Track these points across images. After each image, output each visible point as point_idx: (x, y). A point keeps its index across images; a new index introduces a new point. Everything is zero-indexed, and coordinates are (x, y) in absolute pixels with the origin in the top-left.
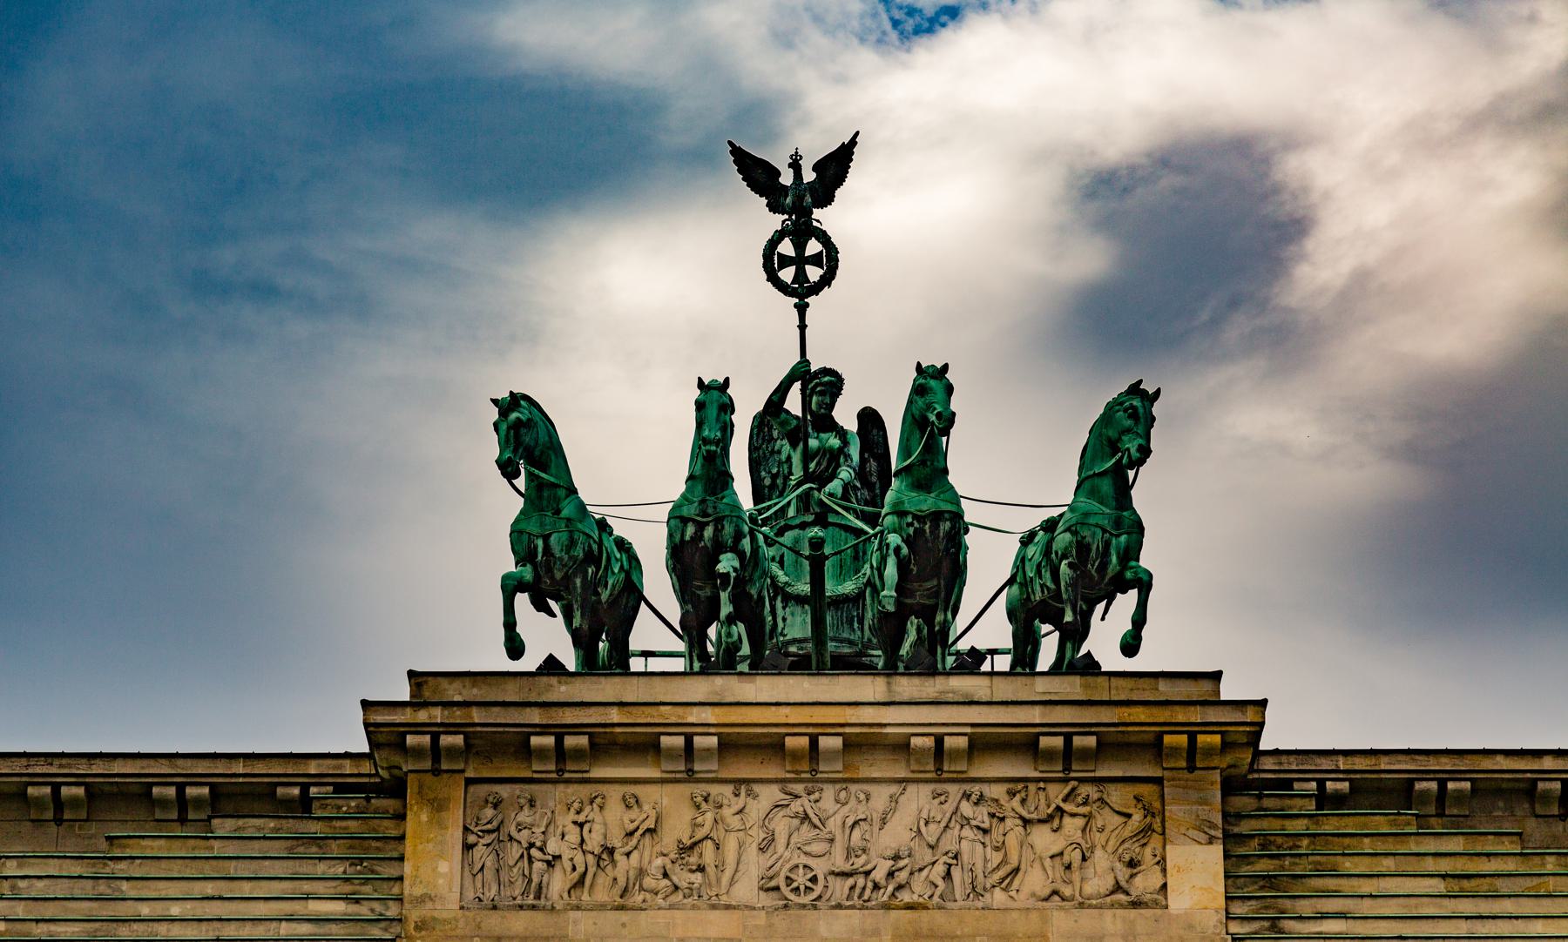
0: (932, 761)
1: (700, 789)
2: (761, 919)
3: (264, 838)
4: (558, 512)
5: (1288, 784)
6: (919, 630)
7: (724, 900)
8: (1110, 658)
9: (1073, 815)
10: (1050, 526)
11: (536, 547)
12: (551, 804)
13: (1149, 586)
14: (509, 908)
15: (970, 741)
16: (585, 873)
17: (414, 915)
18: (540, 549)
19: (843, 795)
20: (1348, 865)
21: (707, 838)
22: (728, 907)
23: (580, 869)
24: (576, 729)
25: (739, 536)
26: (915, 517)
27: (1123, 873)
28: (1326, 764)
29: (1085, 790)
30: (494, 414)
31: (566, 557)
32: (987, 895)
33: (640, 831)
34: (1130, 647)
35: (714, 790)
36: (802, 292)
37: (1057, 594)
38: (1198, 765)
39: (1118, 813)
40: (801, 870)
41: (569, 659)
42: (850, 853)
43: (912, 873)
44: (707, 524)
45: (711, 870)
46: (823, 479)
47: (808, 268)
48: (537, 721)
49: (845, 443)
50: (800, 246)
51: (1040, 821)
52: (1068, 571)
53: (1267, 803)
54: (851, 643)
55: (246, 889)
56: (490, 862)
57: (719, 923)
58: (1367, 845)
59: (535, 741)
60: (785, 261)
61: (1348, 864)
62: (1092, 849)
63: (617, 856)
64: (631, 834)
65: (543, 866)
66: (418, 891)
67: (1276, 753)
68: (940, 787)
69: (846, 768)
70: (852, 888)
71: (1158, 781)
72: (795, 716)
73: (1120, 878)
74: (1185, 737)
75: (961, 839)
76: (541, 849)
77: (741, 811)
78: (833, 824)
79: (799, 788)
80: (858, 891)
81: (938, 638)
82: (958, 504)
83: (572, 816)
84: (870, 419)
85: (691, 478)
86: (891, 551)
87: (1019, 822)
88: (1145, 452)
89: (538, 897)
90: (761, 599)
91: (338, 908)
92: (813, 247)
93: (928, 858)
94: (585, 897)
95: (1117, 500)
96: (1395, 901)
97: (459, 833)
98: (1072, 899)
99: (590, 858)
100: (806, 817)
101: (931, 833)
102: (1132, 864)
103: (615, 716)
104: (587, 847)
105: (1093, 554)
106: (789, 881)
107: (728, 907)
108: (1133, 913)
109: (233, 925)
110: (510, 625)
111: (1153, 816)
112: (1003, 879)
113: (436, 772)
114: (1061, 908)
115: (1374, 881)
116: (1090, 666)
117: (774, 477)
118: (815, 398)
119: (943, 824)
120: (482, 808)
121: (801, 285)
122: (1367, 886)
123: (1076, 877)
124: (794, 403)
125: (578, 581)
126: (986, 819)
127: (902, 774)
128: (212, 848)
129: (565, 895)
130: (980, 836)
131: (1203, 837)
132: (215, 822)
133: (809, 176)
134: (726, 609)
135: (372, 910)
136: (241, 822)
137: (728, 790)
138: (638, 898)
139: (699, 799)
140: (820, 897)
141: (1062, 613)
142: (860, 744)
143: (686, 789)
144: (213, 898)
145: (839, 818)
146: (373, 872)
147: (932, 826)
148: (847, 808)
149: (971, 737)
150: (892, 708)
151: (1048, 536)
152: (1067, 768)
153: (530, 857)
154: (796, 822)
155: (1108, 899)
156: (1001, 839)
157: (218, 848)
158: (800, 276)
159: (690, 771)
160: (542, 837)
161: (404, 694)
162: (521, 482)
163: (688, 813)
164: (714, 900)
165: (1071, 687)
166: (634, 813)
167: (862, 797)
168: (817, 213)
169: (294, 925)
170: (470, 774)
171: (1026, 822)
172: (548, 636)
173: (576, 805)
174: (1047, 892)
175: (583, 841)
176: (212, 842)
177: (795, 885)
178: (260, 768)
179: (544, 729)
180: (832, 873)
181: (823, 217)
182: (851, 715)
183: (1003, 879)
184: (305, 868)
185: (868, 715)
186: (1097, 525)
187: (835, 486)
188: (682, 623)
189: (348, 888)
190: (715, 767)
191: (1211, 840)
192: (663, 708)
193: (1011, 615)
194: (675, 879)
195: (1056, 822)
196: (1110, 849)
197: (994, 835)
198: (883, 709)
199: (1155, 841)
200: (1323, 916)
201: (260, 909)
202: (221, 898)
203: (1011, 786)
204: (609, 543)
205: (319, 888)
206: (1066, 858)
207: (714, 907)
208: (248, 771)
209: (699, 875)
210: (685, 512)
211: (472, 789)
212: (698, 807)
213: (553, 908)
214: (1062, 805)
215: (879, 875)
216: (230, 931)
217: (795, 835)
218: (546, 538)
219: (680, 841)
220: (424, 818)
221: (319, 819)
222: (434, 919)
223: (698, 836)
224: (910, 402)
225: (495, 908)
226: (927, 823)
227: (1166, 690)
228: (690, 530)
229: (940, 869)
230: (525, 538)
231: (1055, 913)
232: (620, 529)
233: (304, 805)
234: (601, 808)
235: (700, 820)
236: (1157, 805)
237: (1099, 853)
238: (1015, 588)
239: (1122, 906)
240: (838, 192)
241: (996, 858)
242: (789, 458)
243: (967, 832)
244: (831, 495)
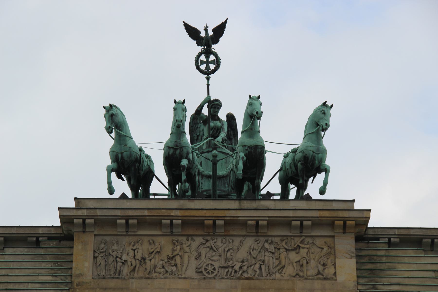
0: (254, 229)
1: (175, 238)
2: (196, 282)
3: (23, 254)
4: (126, 145)
5: (378, 239)
6: (249, 186)
7: (183, 276)
8: (316, 195)
9: (304, 248)
10: (294, 151)
11: (118, 157)
12: (124, 243)
13: (329, 171)
14: (109, 278)
15: (268, 222)
16: (136, 266)
17: (76, 281)
18: (120, 157)
19: (224, 240)
20: (400, 267)
21: (177, 254)
22: (185, 278)
23: (134, 265)
24: (132, 217)
25: (188, 153)
26: (249, 147)
27: (321, 268)
28: (391, 232)
29: (307, 240)
30: (104, 111)
31: (129, 160)
32: (274, 275)
33: (155, 252)
34: (322, 192)
35: (180, 238)
36: (208, 73)
37: (297, 175)
38: (347, 231)
39: (319, 248)
40: (210, 266)
41: (129, 194)
42: (226, 260)
43: (248, 267)
44: (177, 149)
45: (179, 266)
46: (215, 136)
47: (210, 64)
48: (119, 215)
49: (223, 125)
50: (207, 57)
51: (292, 250)
53: (371, 245)
54: (225, 191)
55: (17, 272)
56: (103, 263)
57: (181, 284)
58: (406, 260)
59: (119, 221)
60: (202, 63)
61: (400, 266)
62: (310, 260)
63: (147, 261)
64: (152, 253)
65: (121, 264)
66: (78, 272)
67: (374, 228)
68: (257, 238)
69: (225, 231)
70: (227, 272)
71: (333, 237)
72: (208, 213)
75: (264, 256)
76: (120, 258)
77: (189, 246)
78: (221, 250)
79: (209, 238)
80: (229, 273)
81: (256, 188)
82: (263, 143)
83: (131, 247)
84: (231, 118)
85: (172, 133)
86: (241, 158)
87: (284, 250)
88: (327, 125)
89: (119, 275)
90: (195, 175)
91: (49, 278)
92: (212, 58)
93: (254, 262)
94: (136, 275)
95: (318, 142)
96: (417, 279)
97: (92, 252)
98: (303, 277)
99: (137, 262)
100: (211, 248)
102: (324, 265)
103: (146, 213)
105: (309, 160)
106: (206, 269)
107: (185, 278)
108: (325, 282)
109: (12, 285)
110: (109, 183)
111: (331, 248)
112: (279, 270)
113: (84, 232)
114: (300, 280)
115: (409, 272)
116: (308, 198)
117: (198, 136)
118: (212, 109)
119: (258, 251)
120: (101, 244)
121: (208, 71)
122: (407, 274)
123: (305, 269)
124: (205, 111)
125: (133, 168)
126: (273, 249)
127: (244, 234)
128: (5, 258)
129: (129, 274)
130: (271, 255)
131: (348, 256)
132: (6, 249)
133: (211, 33)
134: (184, 177)
135: (61, 279)
136: (15, 249)
137: (184, 238)
138: (154, 275)
139: (175, 241)
140: (216, 275)
141: (299, 180)
142: (231, 223)
143: (170, 238)
144: (5, 275)
145: (223, 248)
146: (62, 266)
147: (255, 251)
148: (225, 245)
150: (241, 211)
151: (294, 154)
152: (301, 232)
153: (116, 261)
154: (208, 249)
155: (316, 277)
156: (278, 256)
157: (7, 258)
158: (208, 67)
159: (172, 232)
160: (121, 254)
161: (73, 205)
162: (113, 135)
163: (171, 247)
164: (180, 276)
165: (302, 204)
166: (152, 246)
167: (231, 241)
168: (213, 46)
169: (34, 284)
170: (96, 233)
171: (287, 250)
172: (122, 187)
173: (133, 243)
174: (294, 274)
175: (135, 255)
176: (5, 256)
177: (208, 271)
178: (22, 231)
179: (122, 218)
180: (220, 267)
181: (215, 47)
182: (227, 213)
183: (279, 270)
184: (38, 265)
185: (233, 213)
186: (311, 150)
187: (219, 139)
188: (169, 183)
189: (53, 272)
190: (180, 230)
191: (351, 258)
192: (163, 210)
193: (281, 181)
194: (166, 268)
195: (297, 251)
196: (316, 260)
197: (276, 255)
198: (238, 211)
199: (332, 257)
200: (391, 284)
201: (22, 279)
202: (8, 275)
203: (282, 238)
204: (143, 156)
205: (43, 271)
206: (301, 263)
207: (180, 278)
208: (17, 232)
209: (175, 267)
210: (170, 145)
211: (97, 237)
212: (174, 244)
213: (124, 278)
214: (299, 244)
215: (237, 268)
216: (11, 287)
217: (208, 254)
218: (122, 153)
219: (168, 256)
220: (80, 247)
221: (42, 248)
222: (83, 282)
223: (175, 253)
224: (247, 108)
225: (104, 278)
226: (253, 250)
227: (335, 206)
228: (172, 151)
229: (257, 266)
230: (115, 153)
231: (297, 281)
232: (147, 151)
233: (38, 243)
235: (175, 248)
236: (332, 245)
237: (312, 261)
238: (282, 172)
239: (321, 279)
240: (221, 39)
241: (277, 262)
242: (203, 130)
243: (267, 253)
244: (218, 142)
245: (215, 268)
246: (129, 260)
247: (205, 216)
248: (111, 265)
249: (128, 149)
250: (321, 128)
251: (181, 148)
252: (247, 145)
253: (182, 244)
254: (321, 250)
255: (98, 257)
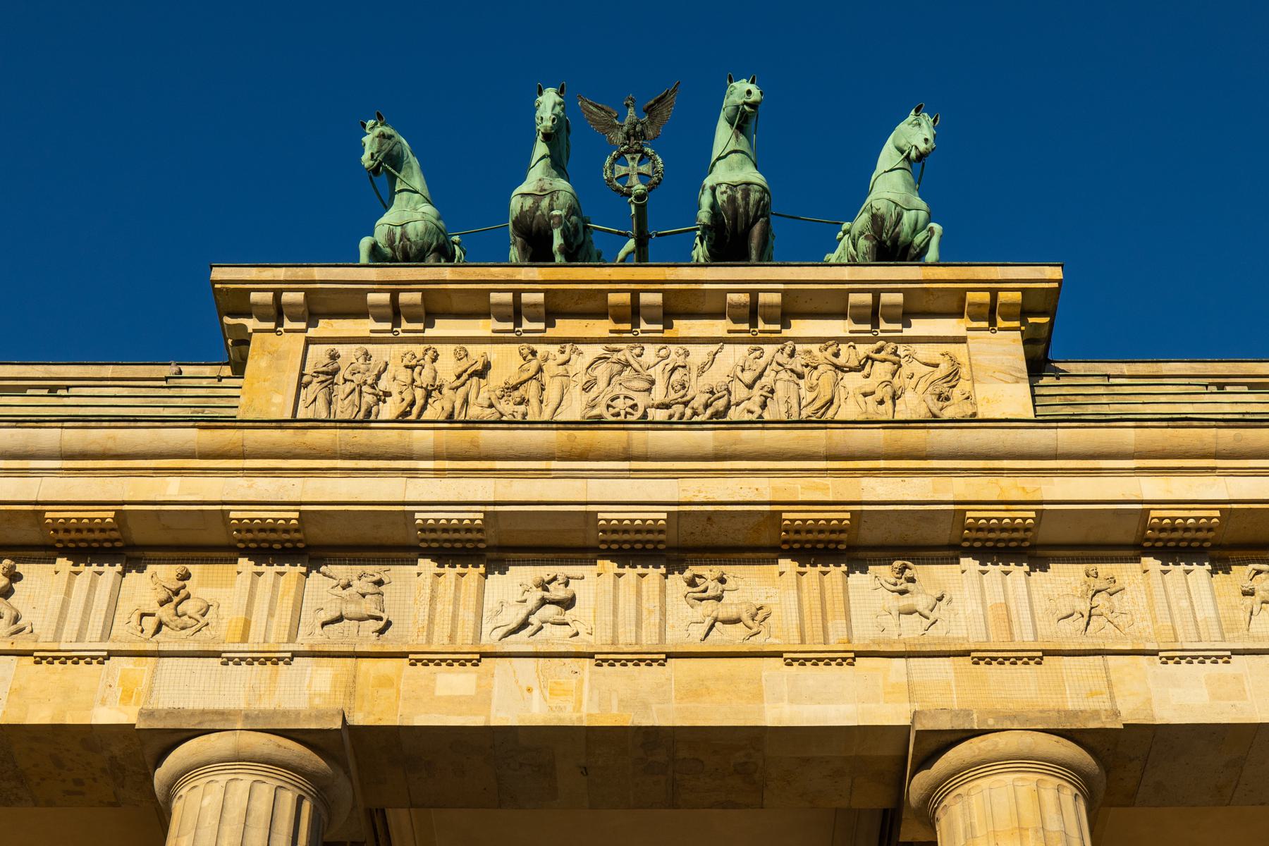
11: (394, 234)
16: (412, 404)
19: (663, 353)
23: (408, 398)
35: (541, 349)
51: (851, 370)
52: (867, 243)
53: (1063, 381)
59: (372, 298)
63: (445, 390)
64: (459, 377)
71: (962, 340)
73: (931, 405)
74: (987, 295)
99: (419, 394)
101: (748, 377)
102: (943, 398)
104: (418, 383)
105: (887, 224)
119: (757, 373)
131: (1008, 378)
137: (554, 349)
143: (515, 347)
149: (784, 293)
153: (361, 392)
154: (617, 367)
170: (312, 332)
175: (414, 381)
179: (380, 286)
194: (498, 406)
199: (964, 386)
223: (525, 376)
226: (743, 370)
229: (757, 399)
234: (434, 360)
241: (809, 396)
243: (784, 375)
245: (636, 405)
246: (395, 389)
247: (610, 282)
248: (346, 402)
249: (419, 216)
250: (913, 154)
251: (552, 193)
252: (727, 181)
253: (546, 360)
254: (931, 369)
255: (310, 382)
